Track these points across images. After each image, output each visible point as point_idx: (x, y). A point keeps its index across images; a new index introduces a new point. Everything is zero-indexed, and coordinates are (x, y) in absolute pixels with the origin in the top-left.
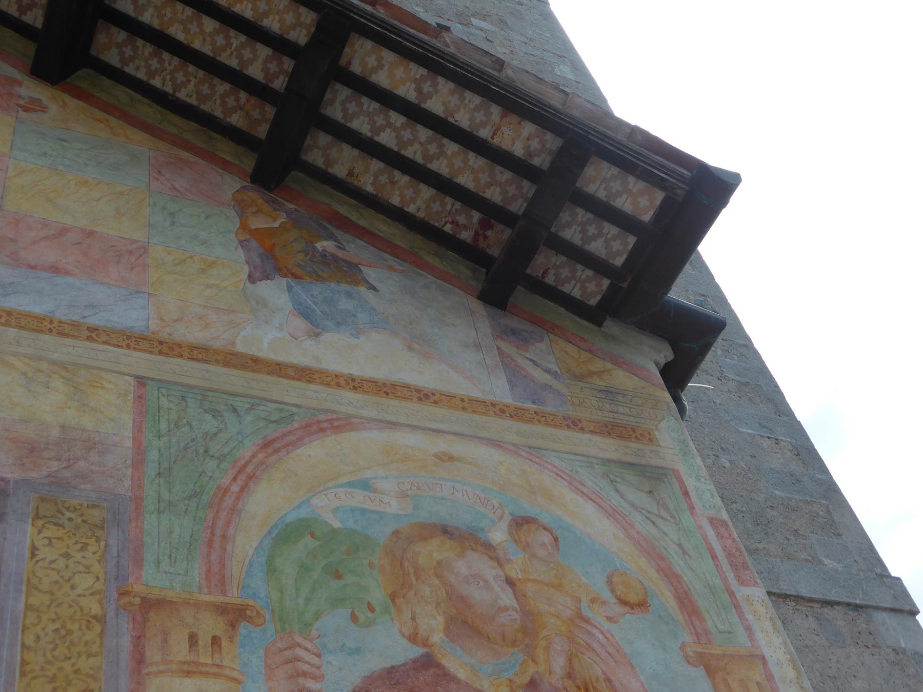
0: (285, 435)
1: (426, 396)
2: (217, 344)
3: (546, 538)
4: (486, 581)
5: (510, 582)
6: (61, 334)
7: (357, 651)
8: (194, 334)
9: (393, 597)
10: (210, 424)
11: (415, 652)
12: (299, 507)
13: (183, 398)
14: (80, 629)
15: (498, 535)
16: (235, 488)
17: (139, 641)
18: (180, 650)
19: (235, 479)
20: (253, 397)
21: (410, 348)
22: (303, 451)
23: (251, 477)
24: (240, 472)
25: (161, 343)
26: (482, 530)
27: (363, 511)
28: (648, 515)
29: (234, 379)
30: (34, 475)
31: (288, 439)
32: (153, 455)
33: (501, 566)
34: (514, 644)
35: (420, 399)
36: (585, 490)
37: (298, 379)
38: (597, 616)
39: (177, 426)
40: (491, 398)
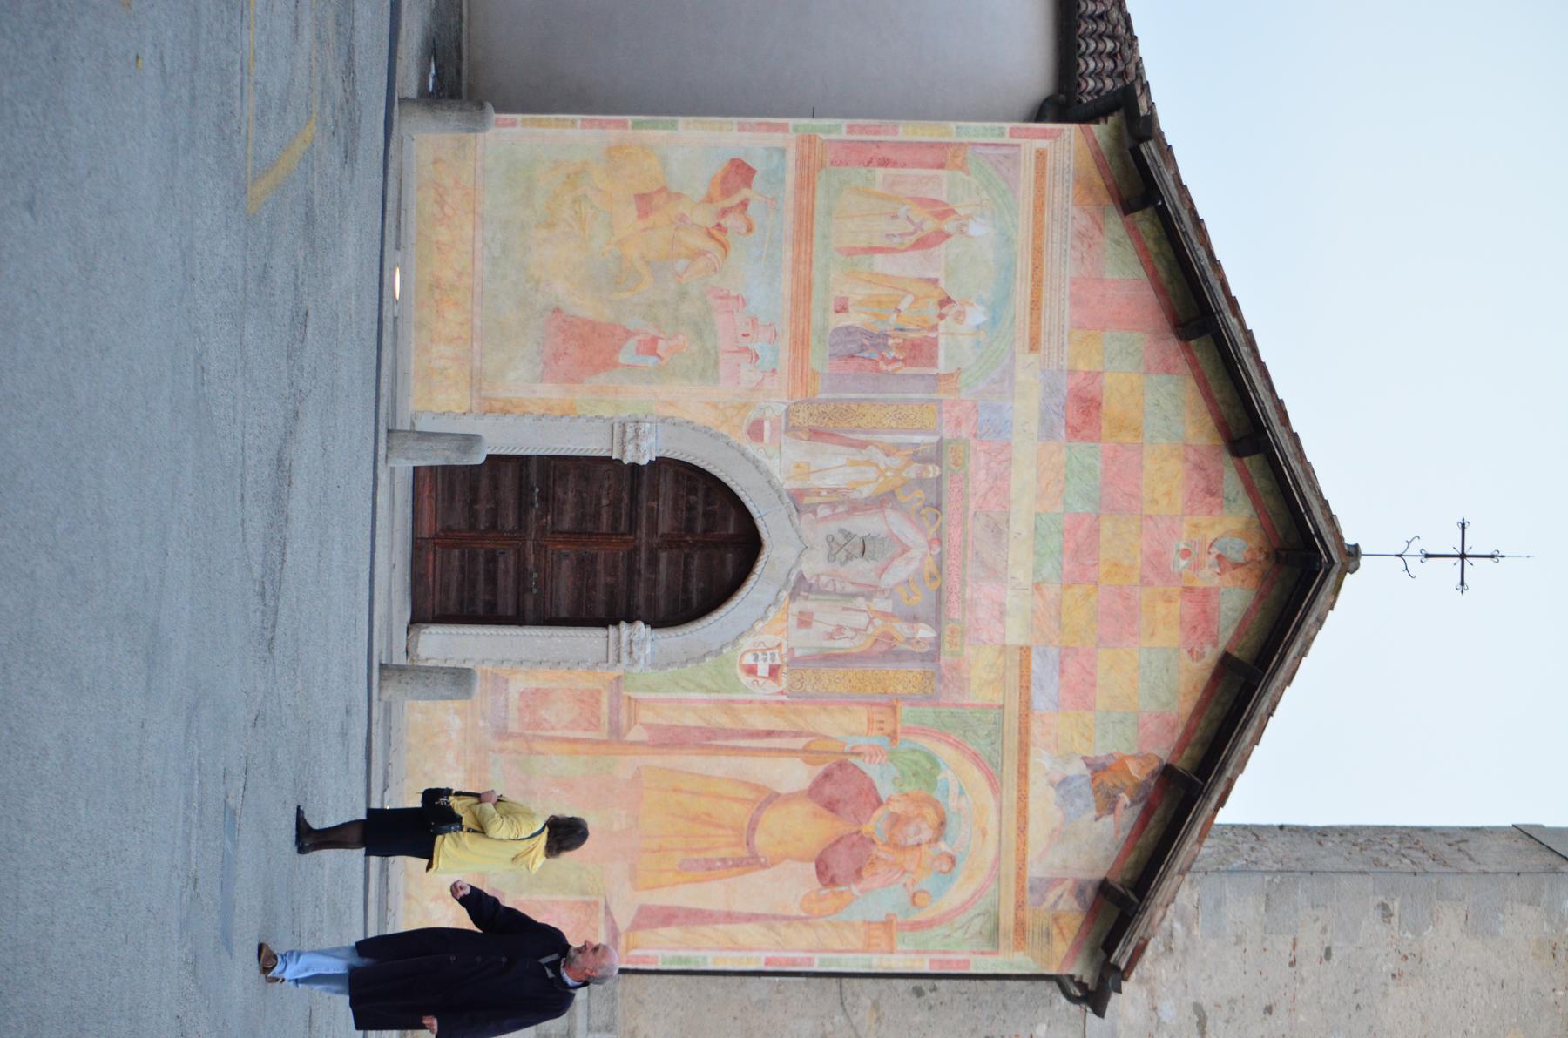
0: (983, 763)
1: (1022, 832)
2: (1032, 738)
3: (945, 868)
4: (918, 834)
5: (919, 845)
6: (1021, 676)
7: (882, 777)
8: (1036, 729)
9: (907, 795)
10: (983, 733)
11: (884, 799)
12: (945, 764)
13: (995, 723)
15: (943, 846)
16: (951, 741)
17: (879, 704)
18: (877, 717)
19: (955, 741)
20: (1002, 752)
21: (1054, 830)
22: (976, 770)
23: (957, 747)
24: (958, 742)
25: (1027, 715)
26: (945, 840)
27: (948, 790)
28: (966, 927)
29: (1012, 742)
30: (944, 669)
31: (981, 764)
32: (961, 711)
33: (927, 843)
34: (890, 838)
35: (1019, 828)
36: (976, 897)
37: (1019, 772)
38: (903, 880)
39: (978, 720)
40: (1028, 866)
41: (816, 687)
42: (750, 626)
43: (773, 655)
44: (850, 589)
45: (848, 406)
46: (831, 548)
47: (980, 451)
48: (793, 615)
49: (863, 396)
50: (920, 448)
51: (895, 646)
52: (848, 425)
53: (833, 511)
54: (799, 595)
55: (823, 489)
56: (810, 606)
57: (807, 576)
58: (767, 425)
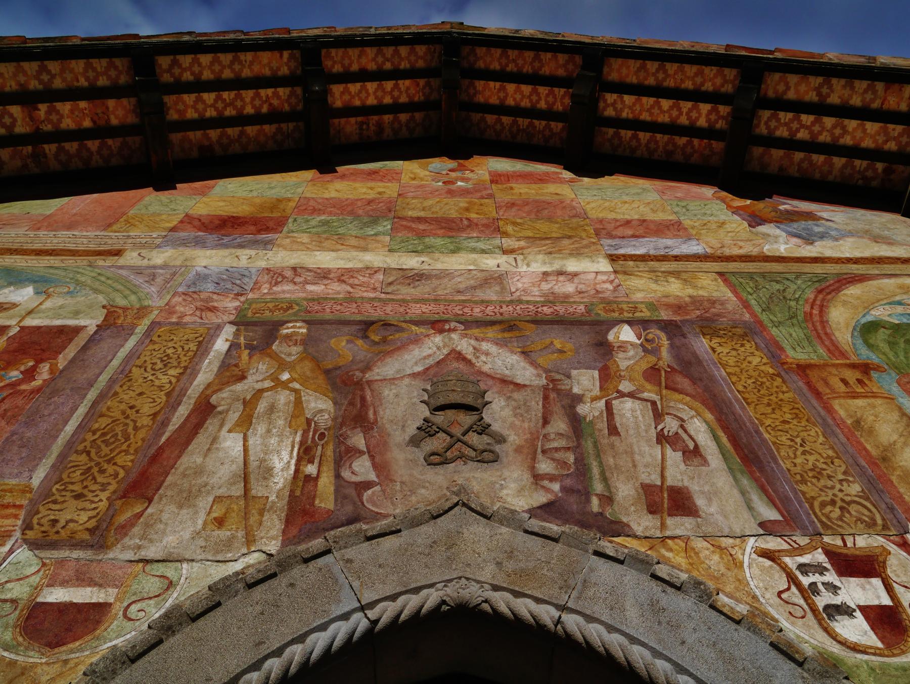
14: (768, 381)
41: (841, 477)
42: (743, 632)
43: (804, 569)
44: (559, 425)
45: (94, 433)
46: (462, 457)
47: (270, 289)
48: (663, 526)
49: (82, 410)
50: (242, 340)
51: (669, 366)
52: (141, 434)
53: (361, 453)
54: (601, 514)
55: (297, 471)
56: (625, 491)
57: (541, 498)
58: (57, 595)
